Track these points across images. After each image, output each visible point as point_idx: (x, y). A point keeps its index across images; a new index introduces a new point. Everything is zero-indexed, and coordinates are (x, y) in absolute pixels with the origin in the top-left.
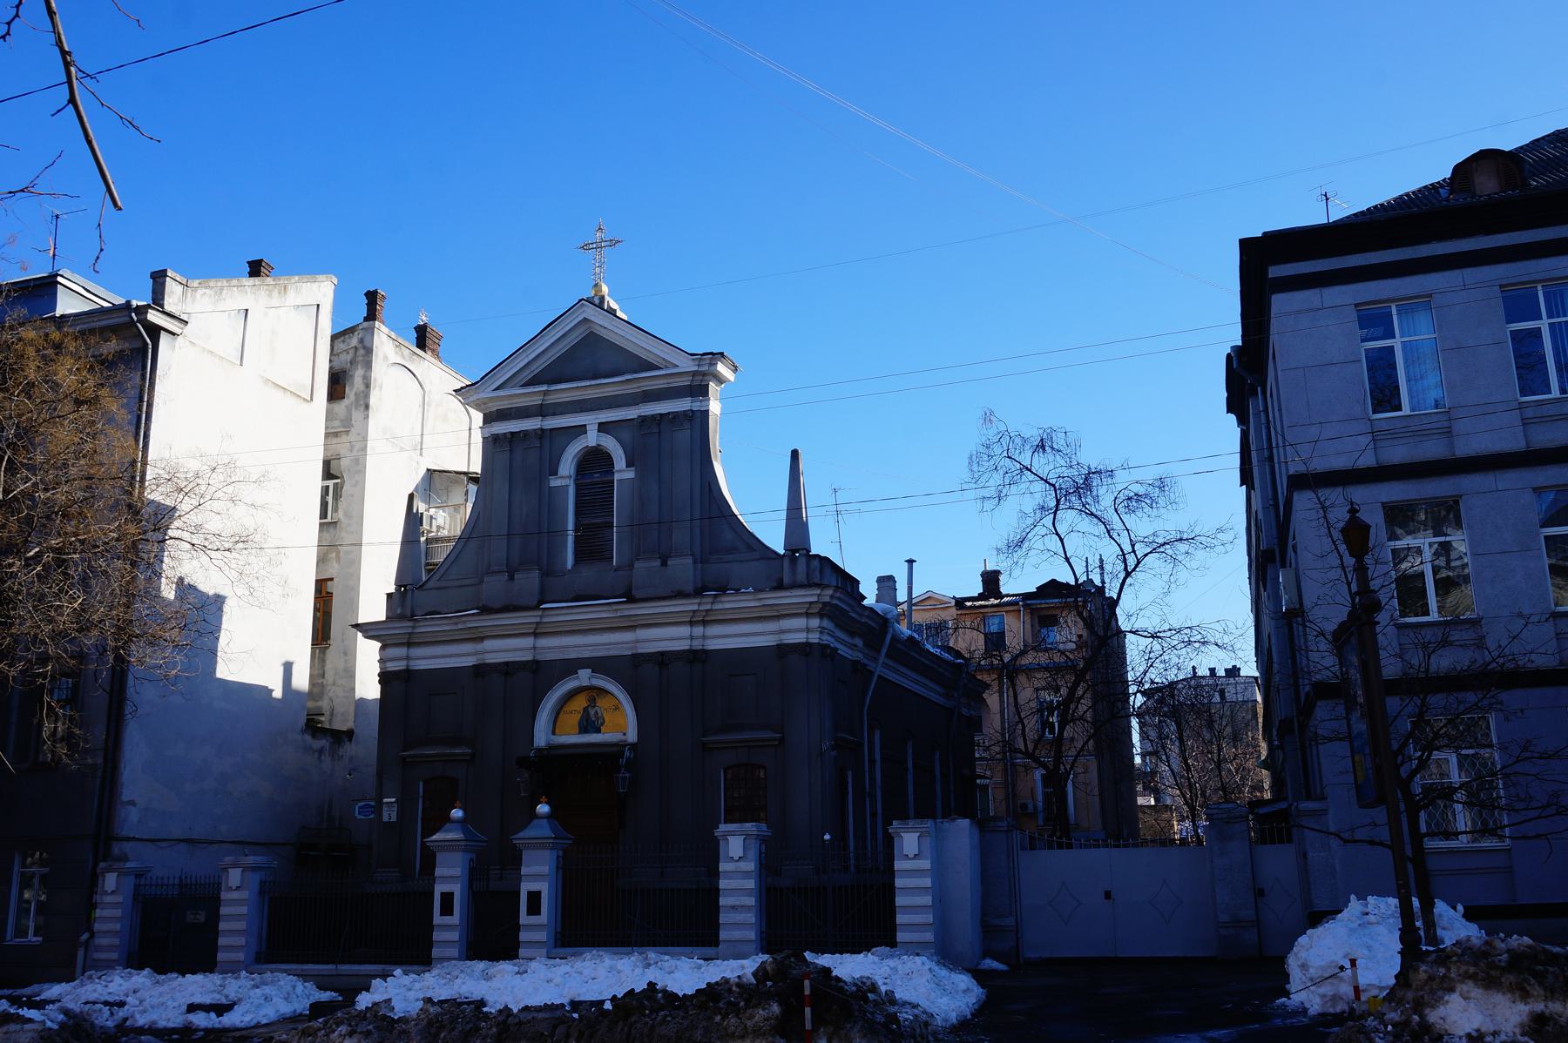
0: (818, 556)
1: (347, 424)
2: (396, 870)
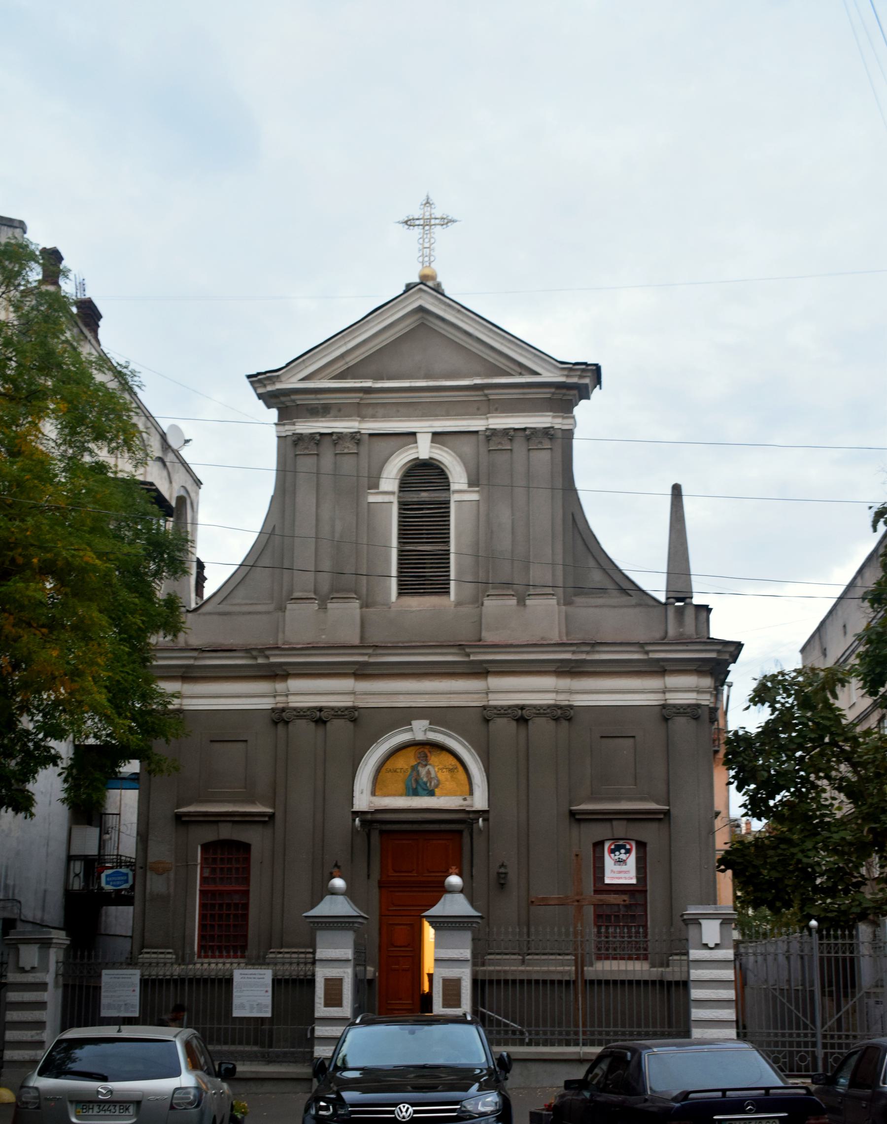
2: (171, 951)
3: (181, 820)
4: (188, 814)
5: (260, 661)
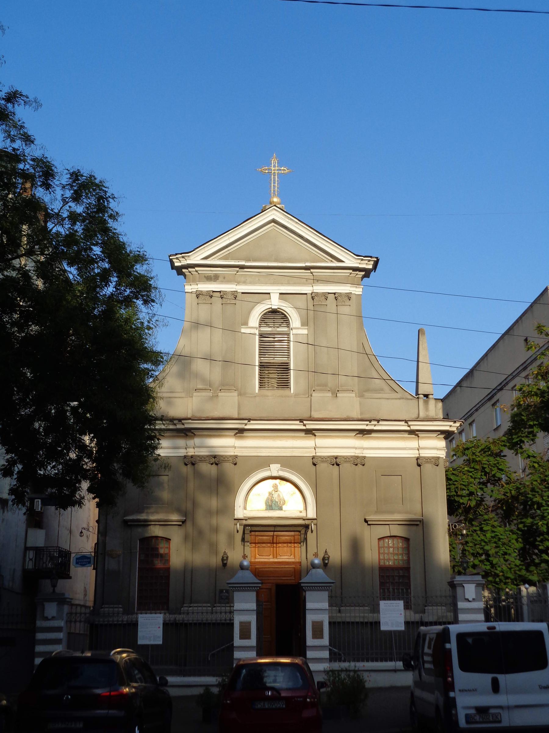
4: (133, 521)
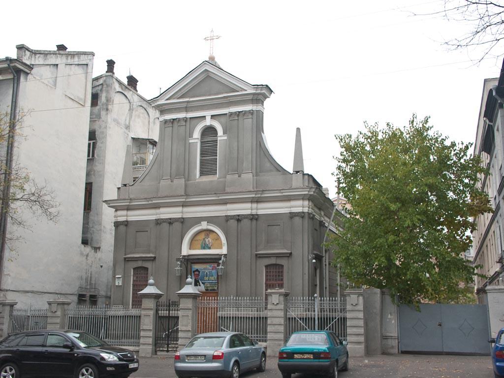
0: (308, 174)
1: (99, 116)
3: (127, 260)
5: (150, 202)
